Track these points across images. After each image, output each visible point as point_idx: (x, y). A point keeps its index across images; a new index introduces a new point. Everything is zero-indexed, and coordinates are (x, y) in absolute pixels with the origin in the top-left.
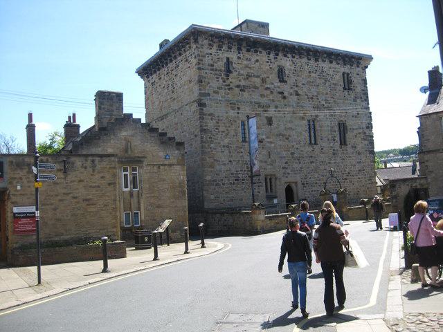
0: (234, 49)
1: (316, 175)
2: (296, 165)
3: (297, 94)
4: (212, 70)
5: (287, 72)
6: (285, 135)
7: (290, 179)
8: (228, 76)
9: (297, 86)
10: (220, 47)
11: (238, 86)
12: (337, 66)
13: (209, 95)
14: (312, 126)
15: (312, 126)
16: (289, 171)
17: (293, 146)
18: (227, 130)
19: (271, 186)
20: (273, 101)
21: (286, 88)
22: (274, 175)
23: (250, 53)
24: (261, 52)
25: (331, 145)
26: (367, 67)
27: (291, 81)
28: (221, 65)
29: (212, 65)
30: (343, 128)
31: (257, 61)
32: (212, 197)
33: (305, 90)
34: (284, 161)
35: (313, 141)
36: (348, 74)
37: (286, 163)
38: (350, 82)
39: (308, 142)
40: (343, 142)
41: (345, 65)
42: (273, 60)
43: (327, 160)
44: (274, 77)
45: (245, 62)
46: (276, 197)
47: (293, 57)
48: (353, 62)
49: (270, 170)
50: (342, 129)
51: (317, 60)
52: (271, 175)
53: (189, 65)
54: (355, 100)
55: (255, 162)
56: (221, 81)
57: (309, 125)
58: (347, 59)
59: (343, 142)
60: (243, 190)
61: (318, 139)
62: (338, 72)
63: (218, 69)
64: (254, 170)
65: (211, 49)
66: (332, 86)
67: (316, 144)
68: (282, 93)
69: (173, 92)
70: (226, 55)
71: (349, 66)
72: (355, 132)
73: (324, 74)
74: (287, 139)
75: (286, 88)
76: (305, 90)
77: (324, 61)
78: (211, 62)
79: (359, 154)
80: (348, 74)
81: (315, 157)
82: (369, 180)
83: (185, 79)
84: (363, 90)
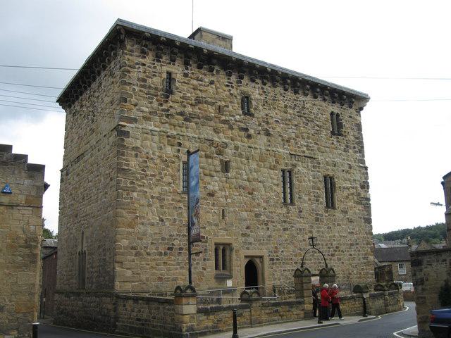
0: (179, 62)
1: (291, 248)
3: (268, 134)
4: (142, 86)
5: (254, 103)
7: (251, 252)
8: (168, 97)
9: (268, 123)
10: (158, 58)
11: (181, 114)
12: (323, 104)
14: (288, 177)
15: (288, 177)
17: (259, 205)
20: (232, 139)
22: (229, 245)
23: (202, 71)
25: (314, 206)
27: (261, 113)
29: (144, 81)
30: (329, 184)
34: (245, 224)
35: (289, 199)
38: (340, 125)
40: (330, 204)
41: (334, 102)
45: (195, 82)
46: (230, 277)
47: (265, 84)
48: (344, 100)
51: (296, 92)
53: (112, 80)
55: (195, 220)
56: (155, 104)
58: (336, 95)
59: (330, 204)
60: (178, 264)
61: (296, 196)
65: (145, 57)
69: (93, 121)
70: (165, 69)
72: (346, 193)
73: (307, 112)
77: (306, 95)
78: (142, 75)
79: (351, 221)
83: (107, 100)
84: (357, 138)
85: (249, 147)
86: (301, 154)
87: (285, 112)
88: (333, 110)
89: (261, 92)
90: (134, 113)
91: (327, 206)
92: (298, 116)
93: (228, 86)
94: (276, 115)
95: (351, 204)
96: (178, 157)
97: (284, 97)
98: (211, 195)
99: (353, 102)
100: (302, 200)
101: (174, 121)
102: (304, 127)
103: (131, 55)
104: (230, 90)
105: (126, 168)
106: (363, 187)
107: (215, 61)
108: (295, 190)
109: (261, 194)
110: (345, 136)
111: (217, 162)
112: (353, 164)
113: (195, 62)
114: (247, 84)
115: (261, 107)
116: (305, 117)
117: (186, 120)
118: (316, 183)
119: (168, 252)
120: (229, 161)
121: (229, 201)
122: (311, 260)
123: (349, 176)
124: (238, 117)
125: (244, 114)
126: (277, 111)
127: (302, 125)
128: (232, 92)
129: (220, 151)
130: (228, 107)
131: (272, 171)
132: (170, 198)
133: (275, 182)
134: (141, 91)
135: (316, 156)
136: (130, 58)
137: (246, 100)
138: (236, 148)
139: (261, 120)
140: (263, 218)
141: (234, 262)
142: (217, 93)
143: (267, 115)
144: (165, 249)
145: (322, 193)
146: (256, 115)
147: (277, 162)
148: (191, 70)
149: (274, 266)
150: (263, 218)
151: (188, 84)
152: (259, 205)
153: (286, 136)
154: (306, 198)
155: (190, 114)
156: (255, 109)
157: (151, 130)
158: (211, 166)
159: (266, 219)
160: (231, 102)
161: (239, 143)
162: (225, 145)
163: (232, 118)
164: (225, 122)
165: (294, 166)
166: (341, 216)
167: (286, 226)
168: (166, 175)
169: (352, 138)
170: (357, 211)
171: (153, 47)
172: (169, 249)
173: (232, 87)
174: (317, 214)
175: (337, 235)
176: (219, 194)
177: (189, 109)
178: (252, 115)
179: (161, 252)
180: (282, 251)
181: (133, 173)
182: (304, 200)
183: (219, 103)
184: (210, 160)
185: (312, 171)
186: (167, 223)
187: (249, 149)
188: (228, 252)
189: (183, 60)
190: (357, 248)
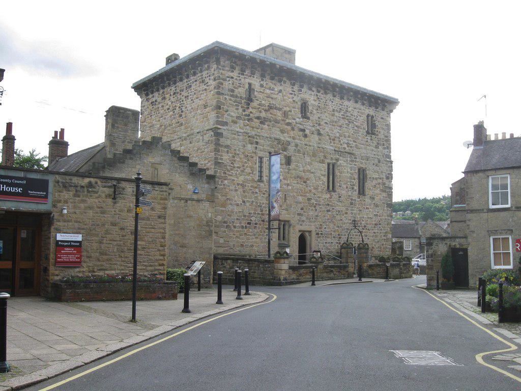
0: (257, 75)
1: (331, 225)
2: (311, 213)
3: (319, 134)
4: (232, 96)
5: (310, 108)
7: (304, 228)
8: (249, 104)
9: (319, 125)
11: (258, 118)
12: (362, 108)
13: (226, 124)
14: (332, 170)
15: (332, 170)
16: (304, 218)
17: (310, 191)
18: (243, 166)
19: (284, 233)
20: (294, 138)
22: (288, 221)
23: (274, 82)
24: (285, 82)
26: (391, 111)
27: (314, 118)
28: (241, 91)
29: (233, 91)
30: (362, 175)
31: (280, 91)
32: (222, 241)
33: (327, 129)
34: (300, 206)
35: (331, 187)
36: (372, 117)
37: (302, 209)
38: (374, 126)
40: (362, 192)
41: (370, 106)
43: (344, 209)
45: (268, 91)
46: (288, 246)
50: (361, 177)
51: (342, 98)
52: (285, 221)
54: (377, 147)
56: (240, 110)
58: (373, 100)
59: (362, 192)
61: (337, 185)
63: (239, 95)
64: (273, 214)
65: (233, 72)
66: (356, 128)
67: (334, 190)
68: (303, 130)
70: (248, 81)
71: (374, 108)
72: (375, 182)
73: (349, 115)
74: (305, 182)
75: (308, 126)
76: (327, 129)
77: (349, 100)
78: (231, 87)
79: (377, 206)
80: (372, 117)
81: (332, 206)
85: (306, 145)
86: (343, 150)
89: (316, 98)
91: (359, 193)
93: (291, 94)
95: (378, 191)
96: (255, 153)
110: (377, 135)
113: (269, 74)
115: (315, 112)
117: (262, 123)
120: (291, 157)
126: (326, 114)
127: (345, 126)
130: (290, 111)
132: (250, 185)
133: (323, 173)
134: (230, 100)
136: (223, 72)
137: (304, 108)
138: (296, 145)
141: (291, 235)
142: (284, 100)
143: (319, 118)
146: (311, 118)
147: (325, 157)
150: (313, 201)
151: (263, 93)
152: (310, 191)
154: (345, 186)
156: (311, 113)
160: (294, 108)
162: (289, 143)
163: (294, 121)
164: (289, 124)
165: (337, 160)
169: (382, 137)
171: (239, 63)
172: (248, 223)
173: (295, 95)
174: (352, 199)
177: (263, 115)
178: (308, 118)
180: (325, 228)
183: (285, 109)
188: (287, 227)
190: (380, 227)
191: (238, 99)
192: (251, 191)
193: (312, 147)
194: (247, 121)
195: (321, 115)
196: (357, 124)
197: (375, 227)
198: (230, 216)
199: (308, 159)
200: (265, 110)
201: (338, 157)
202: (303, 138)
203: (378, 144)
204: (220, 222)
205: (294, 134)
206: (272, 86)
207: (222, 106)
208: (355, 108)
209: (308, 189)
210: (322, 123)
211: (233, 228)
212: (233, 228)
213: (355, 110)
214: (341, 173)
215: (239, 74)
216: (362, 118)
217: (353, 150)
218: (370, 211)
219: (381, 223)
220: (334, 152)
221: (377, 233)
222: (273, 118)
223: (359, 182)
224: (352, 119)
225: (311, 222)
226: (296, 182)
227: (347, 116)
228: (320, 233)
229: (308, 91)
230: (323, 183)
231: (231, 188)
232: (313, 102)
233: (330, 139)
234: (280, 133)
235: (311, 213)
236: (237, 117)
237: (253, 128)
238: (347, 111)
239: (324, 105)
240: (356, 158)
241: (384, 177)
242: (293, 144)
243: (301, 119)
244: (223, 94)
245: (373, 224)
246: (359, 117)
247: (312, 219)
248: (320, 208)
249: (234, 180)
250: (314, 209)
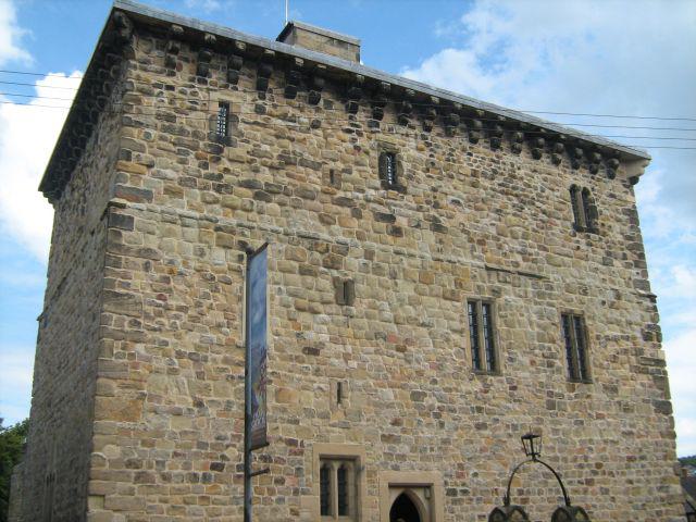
0: (245, 82)
1: (495, 467)
2: (427, 433)
3: (437, 227)
4: (165, 129)
5: (406, 166)
6: (396, 340)
7: (403, 477)
8: (221, 150)
9: (436, 206)
11: (248, 185)
12: (554, 170)
13: (147, 195)
14: (482, 317)
15: (482, 317)
16: (403, 449)
17: (420, 373)
18: (199, 305)
20: (360, 237)
21: (405, 210)
22: (354, 459)
23: (295, 102)
24: (328, 105)
25: (543, 378)
26: (634, 180)
27: (422, 186)
29: (171, 118)
30: (575, 329)
34: (389, 414)
35: (485, 355)
36: (585, 192)
37: (396, 423)
38: (591, 213)
39: (470, 364)
40: (579, 372)
41: (576, 167)
42: (364, 128)
44: (366, 175)
47: (428, 129)
48: (597, 162)
49: (340, 444)
50: (574, 335)
51: (495, 146)
56: (193, 164)
57: (474, 315)
58: (580, 152)
59: (579, 372)
61: (502, 356)
62: (555, 182)
63: (189, 129)
65: (173, 74)
66: (545, 218)
67: (494, 368)
68: (391, 218)
71: (586, 172)
72: (612, 348)
73: (520, 184)
75: (405, 210)
77: (517, 151)
79: (627, 409)
80: (585, 192)
81: (490, 413)
82: (660, 489)
84: (629, 238)
85: (397, 253)
86: (511, 269)
87: (474, 185)
88: (575, 182)
89: (421, 144)
90: (146, 181)
91: (573, 377)
92: (502, 192)
93: (349, 131)
94: (455, 189)
95: (625, 371)
97: (470, 154)
98: (313, 351)
99: (616, 167)
100: (516, 364)
101: (233, 199)
102: (514, 215)
103: (145, 70)
104: (354, 140)
105: (123, 291)
106: (647, 337)
107: (321, 82)
108: (500, 344)
109: (424, 350)
110: (604, 234)
111: (326, 283)
112: (626, 291)
113: (280, 85)
114: (390, 130)
115: (421, 175)
116: (516, 196)
117: (258, 196)
118: (544, 329)
119: (213, 473)
120: (353, 282)
121: (354, 364)
122: (540, 493)
123: (615, 314)
124: (372, 192)
125: (386, 186)
126: (455, 182)
127: (510, 210)
128: (358, 143)
129: (333, 260)
130: (349, 171)
131: (448, 302)
133: (456, 325)
134: (162, 138)
135: (543, 274)
136: (143, 74)
137: (389, 161)
138: (369, 255)
139: (422, 199)
140: (429, 401)
141: (365, 498)
142: (328, 144)
143: (434, 190)
144: (204, 467)
145: (560, 349)
146: (410, 189)
147: (459, 284)
148: (272, 99)
149: (457, 508)
150: (429, 401)
151: (264, 126)
153: (477, 233)
154: (526, 360)
155: (267, 184)
156: (410, 177)
157: (180, 216)
158: (313, 292)
159: (437, 404)
160: (357, 163)
161: (376, 246)
162: (344, 249)
163: (361, 195)
164: (343, 202)
165: (497, 292)
166: (604, 397)
167: (482, 418)
168: (210, 307)
169: (620, 238)
170: (639, 387)
171: (192, 55)
172: (214, 467)
174: (550, 394)
175: (597, 438)
176: (331, 349)
177: (265, 176)
178: (403, 190)
179: (195, 475)
180: (476, 475)
181: (136, 304)
182: (521, 363)
183: (332, 165)
184: (309, 279)
185: (536, 303)
186: (212, 411)
187: (398, 258)
188: (351, 476)
189: (254, 80)
190: (643, 466)
191: (187, 139)
192: (223, 374)
193: (418, 262)
194: (212, 192)
195: (440, 183)
196: (544, 207)
197: (628, 467)
198: (152, 445)
199: (407, 290)
200: (271, 167)
201: (497, 284)
202: (390, 238)
203: (609, 254)
204: (114, 463)
205: (360, 226)
206: (291, 111)
207: (135, 154)
208: (535, 171)
209: (410, 369)
210: (444, 202)
211: (158, 481)
212: (158, 481)
213: (536, 175)
214: (509, 325)
215: (192, 80)
216: (556, 193)
217: (540, 269)
218: (609, 424)
219: (644, 453)
220: (485, 273)
221: (639, 481)
222: (294, 185)
223: (569, 349)
224: (531, 195)
225: (428, 458)
226: (372, 349)
227: (514, 188)
228: (459, 488)
229: (397, 127)
230: (457, 353)
231: (155, 364)
232: (413, 153)
233: (471, 240)
234: (318, 223)
235: (427, 433)
236: (182, 181)
237: (234, 208)
238: (514, 177)
239: (448, 160)
240: (552, 288)
241: (639, 335)
242: (360, 251)
243: (382, 191)
244: (139, 124)
245: (622, 459)
246: (547, 192)
247: (432, 449)
248: (454, 419)
249: (166, 344)
250: (435, 422)
